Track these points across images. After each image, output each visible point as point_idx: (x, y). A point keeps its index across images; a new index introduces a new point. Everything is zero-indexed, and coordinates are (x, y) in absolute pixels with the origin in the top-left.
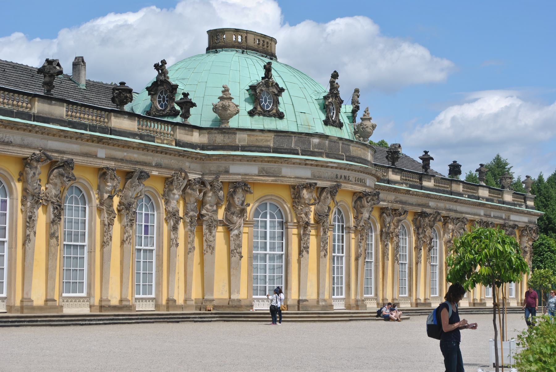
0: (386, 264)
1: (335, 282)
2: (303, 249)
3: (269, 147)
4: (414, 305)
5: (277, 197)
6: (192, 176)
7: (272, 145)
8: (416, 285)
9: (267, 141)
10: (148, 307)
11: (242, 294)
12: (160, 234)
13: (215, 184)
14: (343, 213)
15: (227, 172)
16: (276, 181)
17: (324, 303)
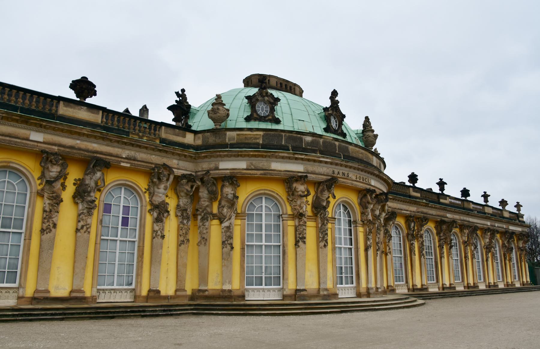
0: (413, 259)
1: (343, 271)
2: (300, 239)
3: (258, 144)
4: (441, 289)
5: (270, 191)
7: (261, 142)
8: (442, 274)
9: (256, 139)
10: (124, 298)
11: (235, 285)
12: (142, 226)
13: (205, 179)
14: (349, 209)
15: (217, 169)
16: (265, 174)
17: (325, 293)
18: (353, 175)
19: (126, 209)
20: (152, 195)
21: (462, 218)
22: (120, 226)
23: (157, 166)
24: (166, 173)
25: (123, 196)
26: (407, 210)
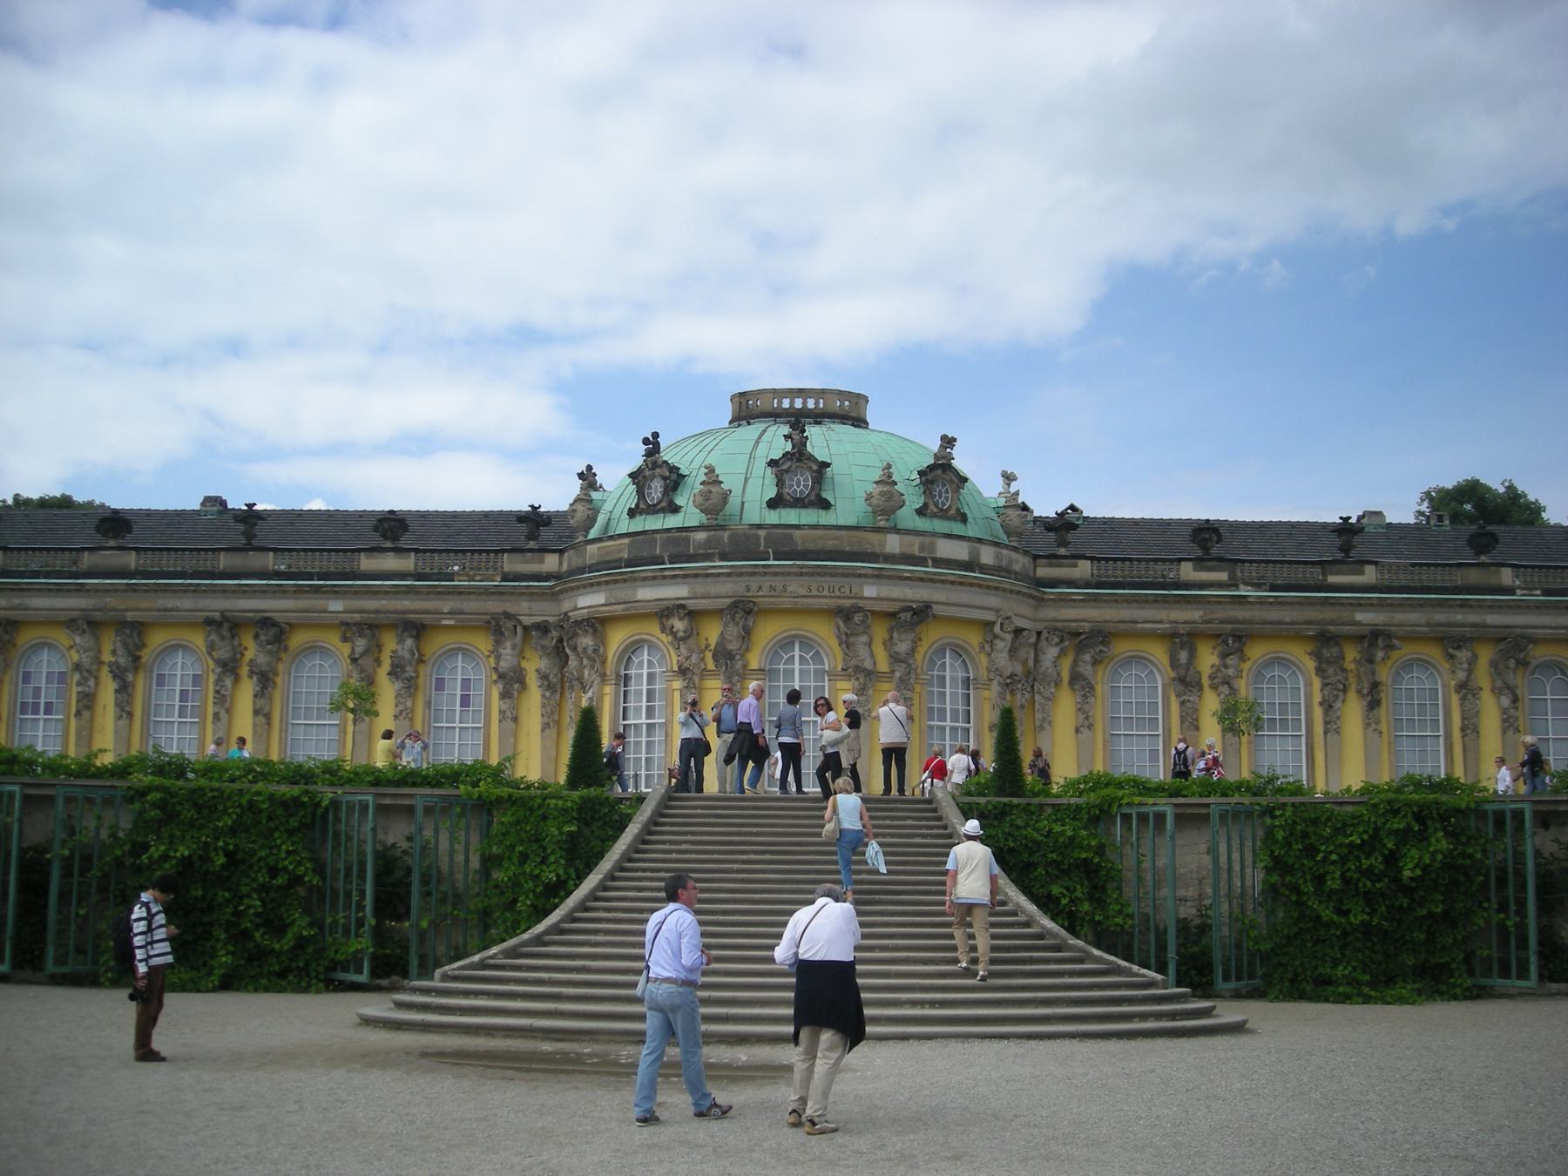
3: (619, 560)
6: (527, 621)
9: (621, 551)
18: (795, 586)
19: (466, 683)
20: (498, 658)
21: (1440, 617)
22: (458, 708)
23: (495, 617)
24: (510, 624)
25: (460, 664)
26: (1160, 622)
